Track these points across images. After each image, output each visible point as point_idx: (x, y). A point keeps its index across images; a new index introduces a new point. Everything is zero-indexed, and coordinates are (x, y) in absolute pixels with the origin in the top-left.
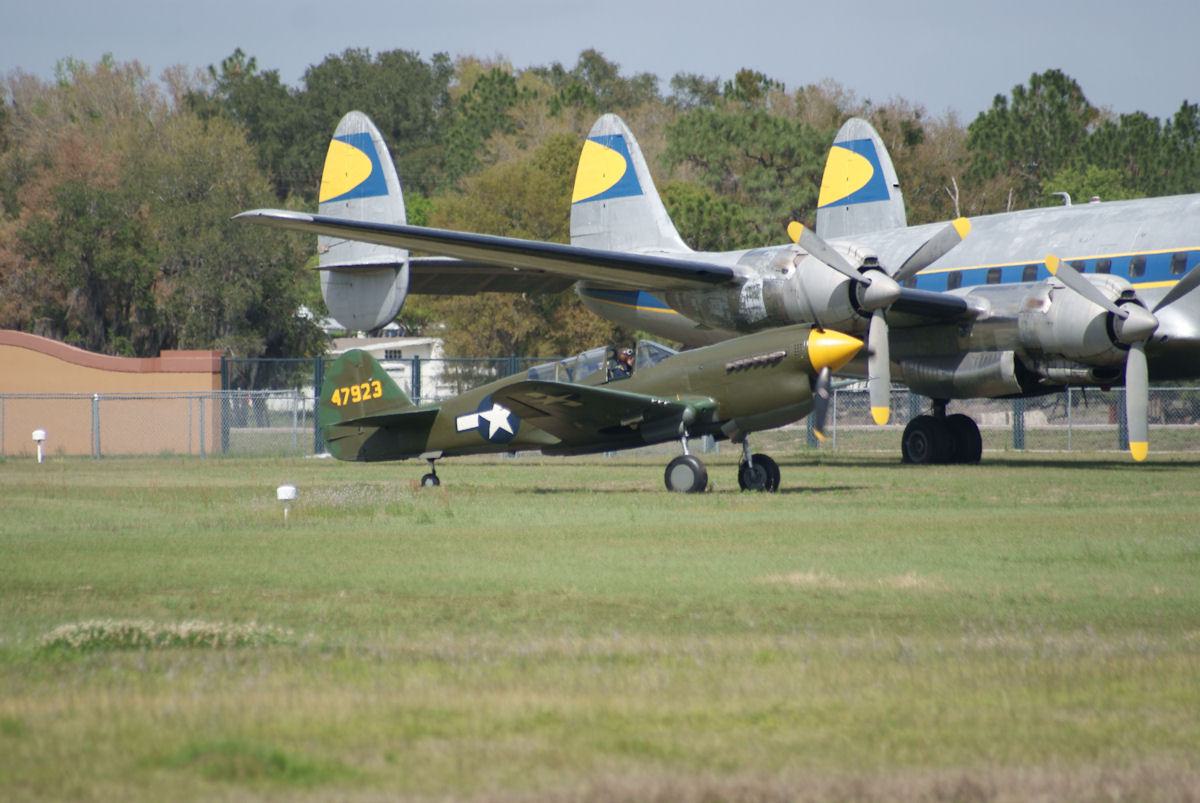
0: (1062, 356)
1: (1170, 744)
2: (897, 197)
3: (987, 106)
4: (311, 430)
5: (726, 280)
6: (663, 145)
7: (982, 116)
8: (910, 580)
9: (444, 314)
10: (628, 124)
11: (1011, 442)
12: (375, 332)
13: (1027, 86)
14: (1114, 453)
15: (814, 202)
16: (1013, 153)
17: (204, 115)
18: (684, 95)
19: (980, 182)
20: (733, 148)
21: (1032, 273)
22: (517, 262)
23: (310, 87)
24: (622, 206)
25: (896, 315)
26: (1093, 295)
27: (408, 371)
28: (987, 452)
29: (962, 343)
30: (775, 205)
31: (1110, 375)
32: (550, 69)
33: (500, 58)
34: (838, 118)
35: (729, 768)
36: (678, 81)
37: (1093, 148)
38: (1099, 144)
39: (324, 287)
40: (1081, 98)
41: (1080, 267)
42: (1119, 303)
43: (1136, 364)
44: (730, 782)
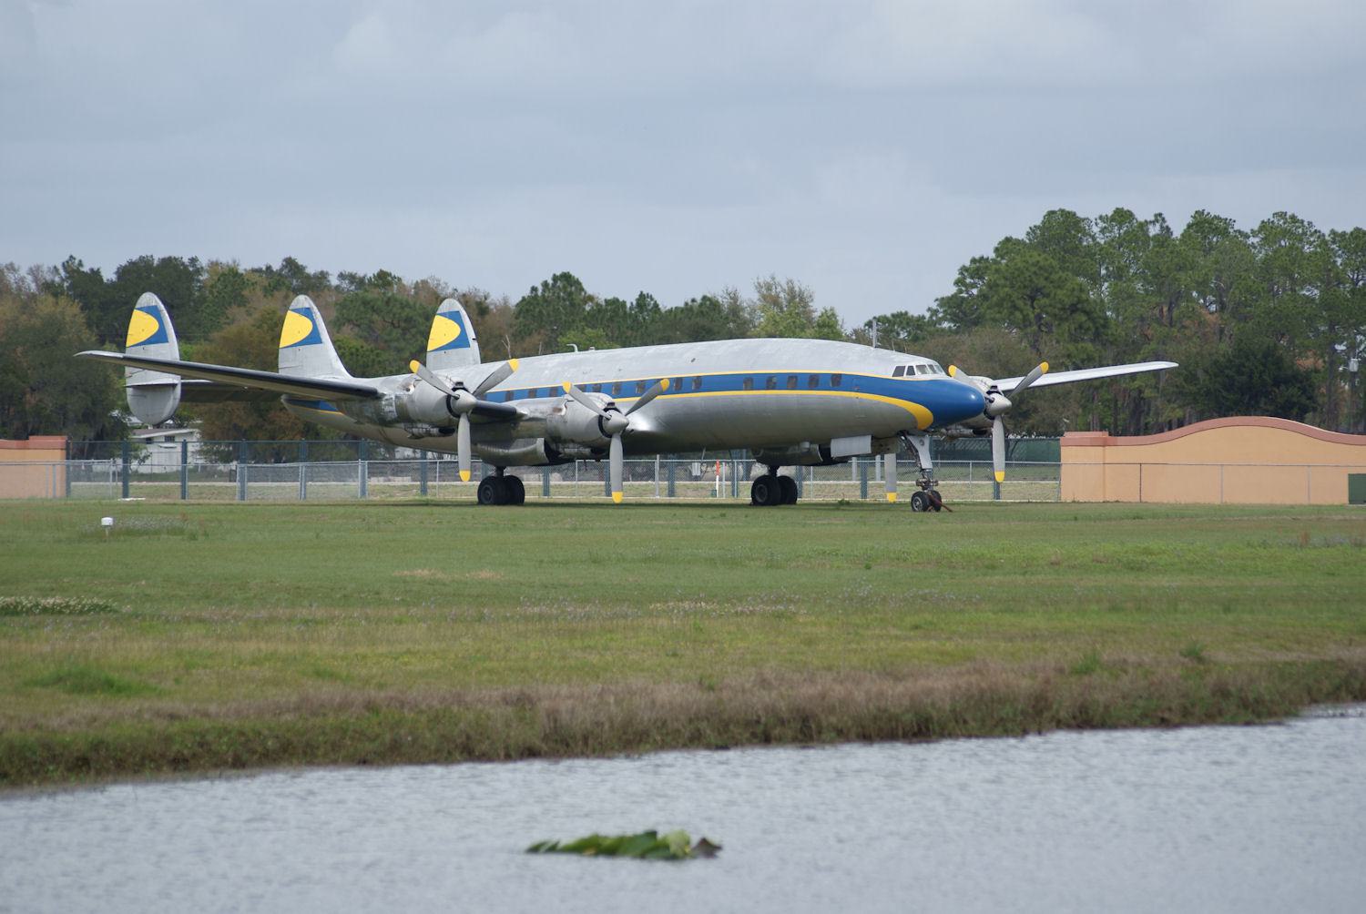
0: (573, 441)
1: (642, 670)
2: (475, 346)
3: (527, 293)
4: (120, 484)
5: (373, 395)
6: (334, 314)
7: (524, 299)
8: (486, 574)
9: (200, 416)
10: (314, 301)
11: (541, 492)
12: (158, 426)
13: (550, 282)
14: (603, 499)
15: (423, 349)
16: (542, 320)
17: (55, 295)
18: (345, 284)
19: (522, 338)
20: (375, 317)
21: (555, 392)
22: (247, 384)
23: (119, 278)
24: (309, 352)
25: (474, 416)
26: (590, 406)
27: (179, 448)
28: (528, 498)
29: (514, 433)
30: (399, 350)
31: (601, 452)
32: (264, 269)
33: (234, 262)
34: (439, 299)
35: (381, 686)
36: (342, 276)
37: (589, 319)
38: (593, 316)
39: (129, 398)
40: (582, 289)
41: (583, 388)
42: (606, 410)
43: (616, 447)
44: (382, 694)
